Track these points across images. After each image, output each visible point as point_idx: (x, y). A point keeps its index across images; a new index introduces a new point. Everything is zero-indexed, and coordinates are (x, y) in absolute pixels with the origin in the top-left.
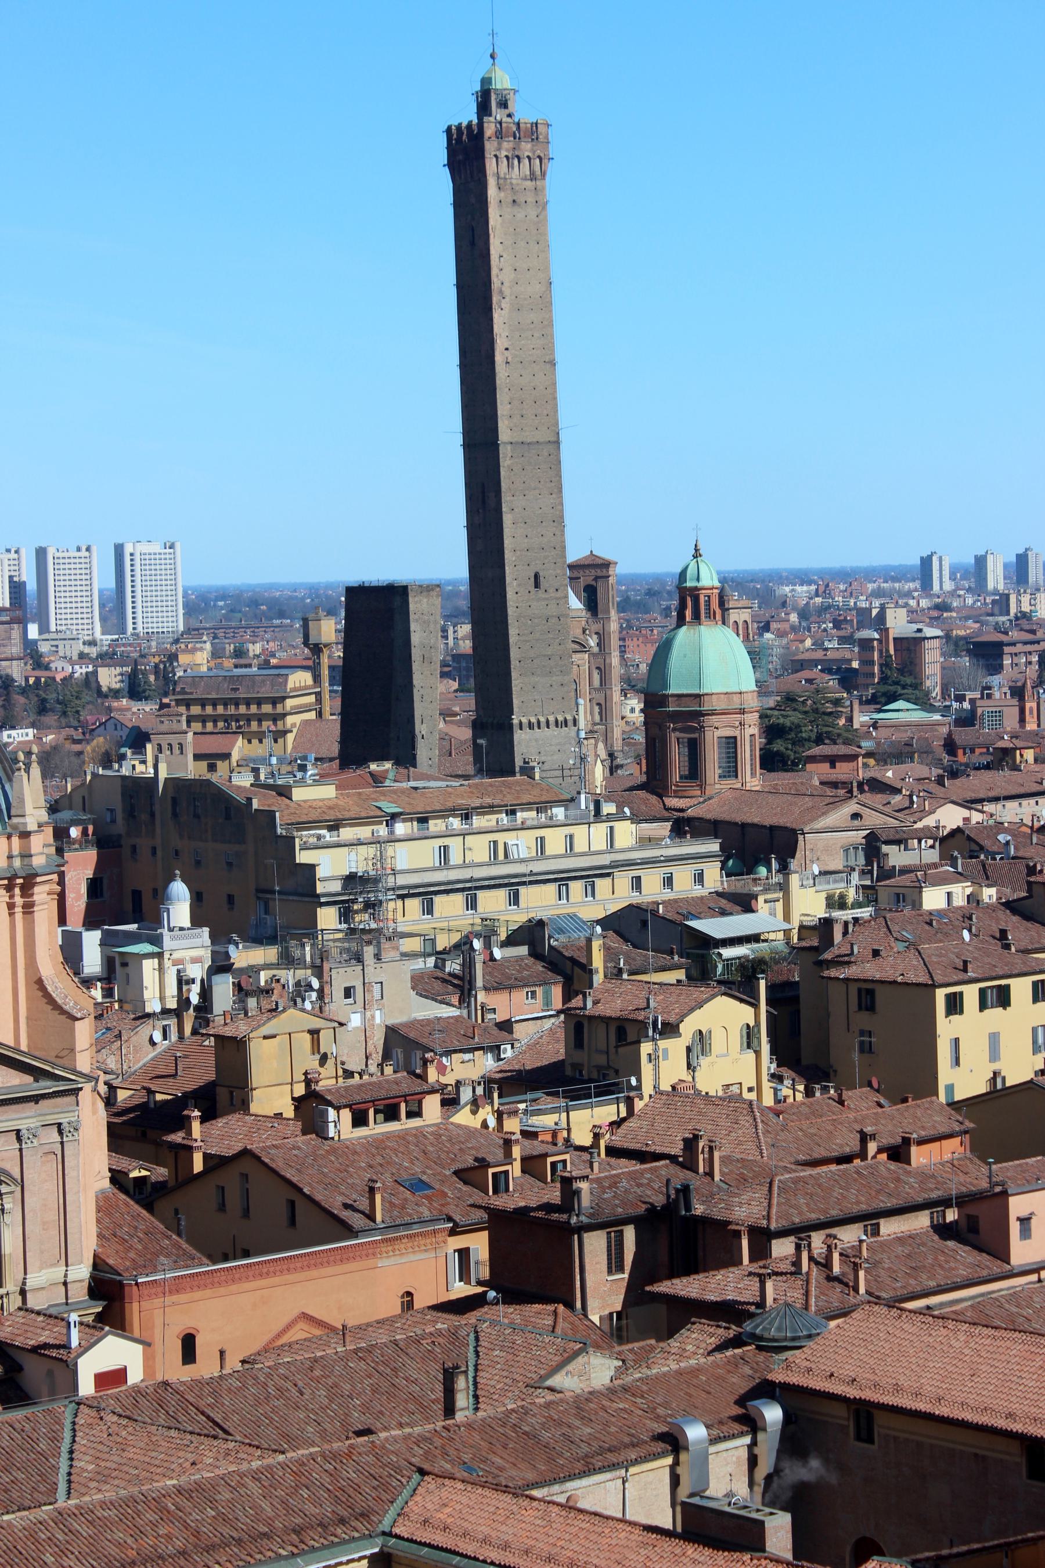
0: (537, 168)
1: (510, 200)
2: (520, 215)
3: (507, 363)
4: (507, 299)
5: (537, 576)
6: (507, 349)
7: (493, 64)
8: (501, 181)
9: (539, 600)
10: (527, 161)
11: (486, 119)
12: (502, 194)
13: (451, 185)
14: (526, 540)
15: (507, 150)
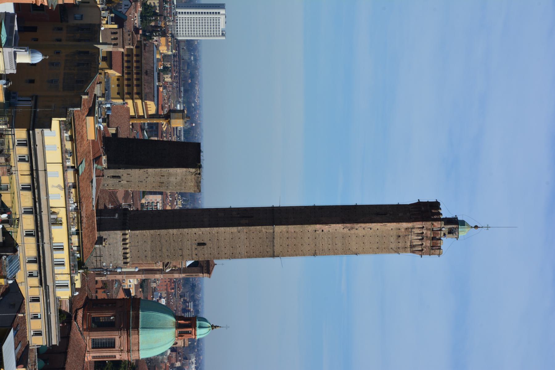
0: (416, 249)
1: (400, 234)
2: (392, 239)
3: (316, 231)
4: (348, 231)
5: (204, 244)
6: (323, 231)
7: (472, 227)
8: (410, 230)
9: (191, 245)
10: (420, 243)
11: (443, 222)
12: (403, 230)
13: (408, 203)
14: (223, 239)
15: (426, 233)
